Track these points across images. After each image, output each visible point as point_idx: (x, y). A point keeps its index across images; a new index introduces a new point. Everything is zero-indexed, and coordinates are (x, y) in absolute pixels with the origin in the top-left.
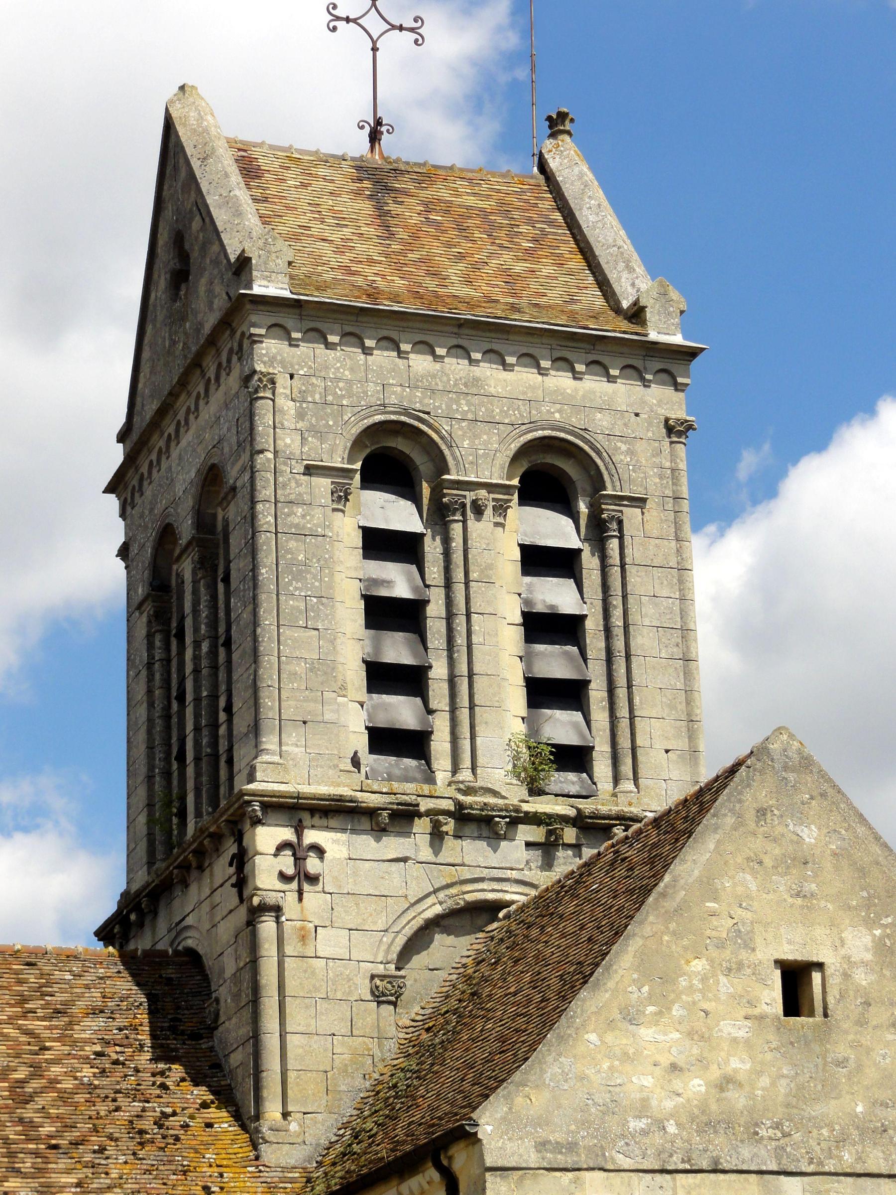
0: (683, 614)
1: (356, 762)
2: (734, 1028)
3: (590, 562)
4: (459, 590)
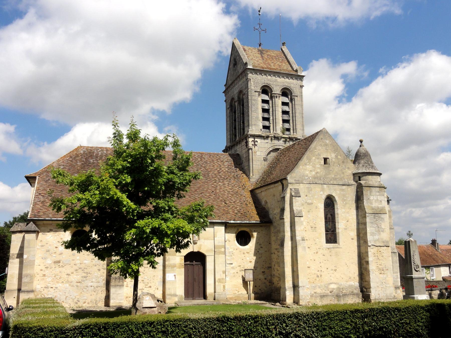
0: (302, 111)
1: (261, 130)
2: (318, 166)
3: (290, 104)
4: (274, 108)
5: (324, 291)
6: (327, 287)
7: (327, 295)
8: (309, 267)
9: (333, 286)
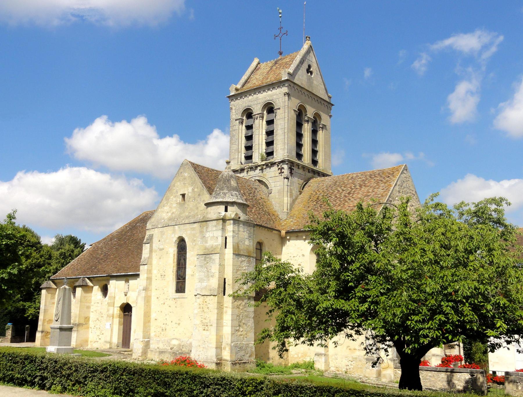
2: (175, 205)
5: (165, 347)
6: (169, 343)
7: (165, 352)
8: (156, 320)
9: (175, 342)
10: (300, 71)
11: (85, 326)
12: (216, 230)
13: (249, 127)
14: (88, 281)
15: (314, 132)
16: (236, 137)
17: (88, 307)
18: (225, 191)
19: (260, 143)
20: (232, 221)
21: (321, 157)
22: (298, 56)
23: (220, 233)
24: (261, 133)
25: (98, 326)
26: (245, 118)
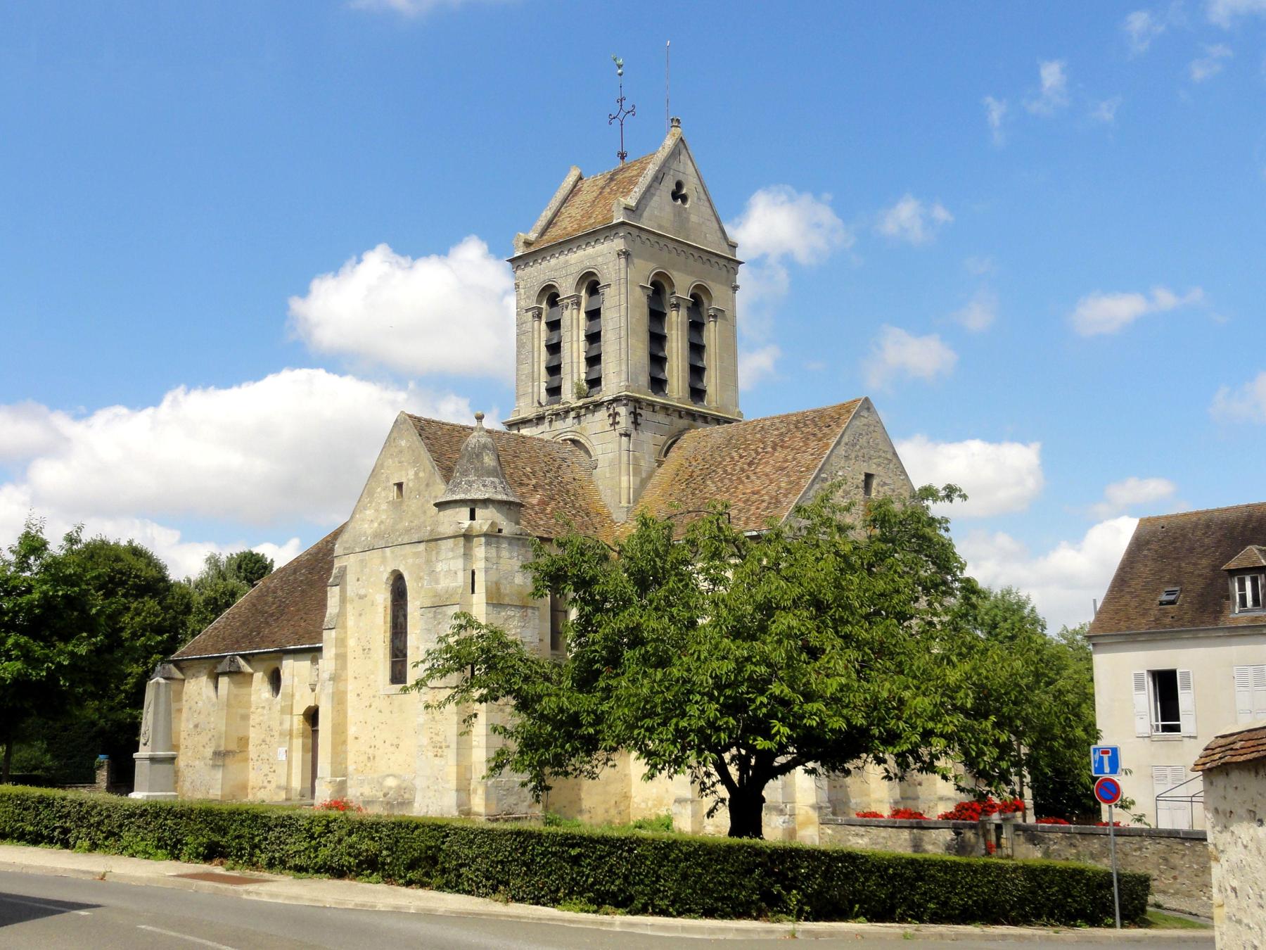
2: (384, 507)
9: (391, 782)
10: (655, 198)
11: (239, 756)
12: (453, 558)
13: (554, 325)
14: (242, 662)
15: (696, 327)
16: (529, 347)
17: (245, 718)
18: (472, 478)
19: (575, 360)
20: (483, 539)
21: (713, 380)
22: (651, 166)
23: (459, 564)
24: (575, 338)
25: (265, 756)
26: (544, 305)
